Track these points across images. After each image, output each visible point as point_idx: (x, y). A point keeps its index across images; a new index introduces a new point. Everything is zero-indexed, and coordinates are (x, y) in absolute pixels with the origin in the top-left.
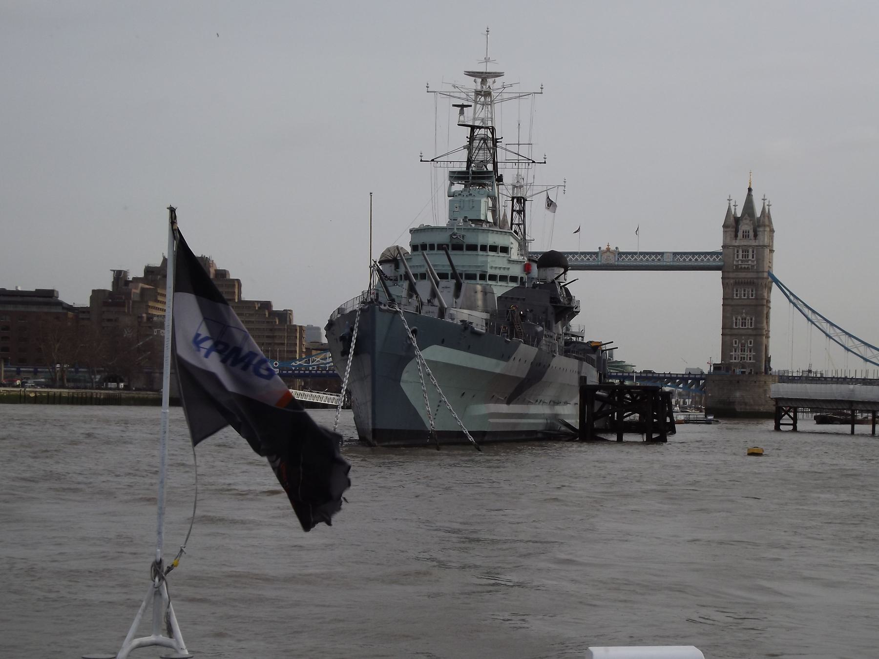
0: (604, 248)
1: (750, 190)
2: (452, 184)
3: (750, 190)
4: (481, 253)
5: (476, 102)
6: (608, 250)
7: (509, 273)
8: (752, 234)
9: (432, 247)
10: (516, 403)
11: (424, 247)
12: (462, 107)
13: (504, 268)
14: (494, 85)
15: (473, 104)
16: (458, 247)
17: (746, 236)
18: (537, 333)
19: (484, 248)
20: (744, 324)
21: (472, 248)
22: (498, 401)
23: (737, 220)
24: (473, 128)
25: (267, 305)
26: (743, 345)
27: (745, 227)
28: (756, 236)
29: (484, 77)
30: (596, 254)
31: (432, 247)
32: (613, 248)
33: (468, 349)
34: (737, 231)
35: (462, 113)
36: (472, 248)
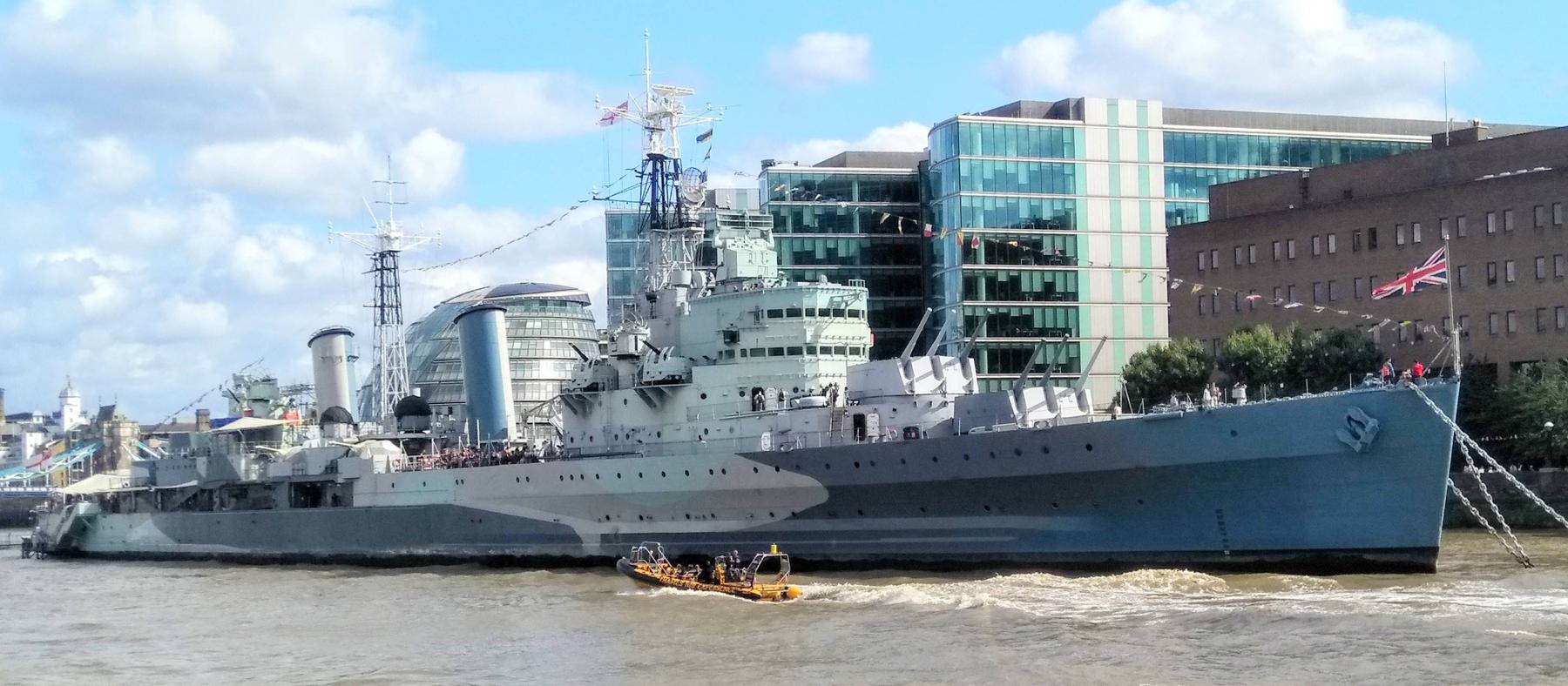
16: (839, 313)
31: (810, 313)
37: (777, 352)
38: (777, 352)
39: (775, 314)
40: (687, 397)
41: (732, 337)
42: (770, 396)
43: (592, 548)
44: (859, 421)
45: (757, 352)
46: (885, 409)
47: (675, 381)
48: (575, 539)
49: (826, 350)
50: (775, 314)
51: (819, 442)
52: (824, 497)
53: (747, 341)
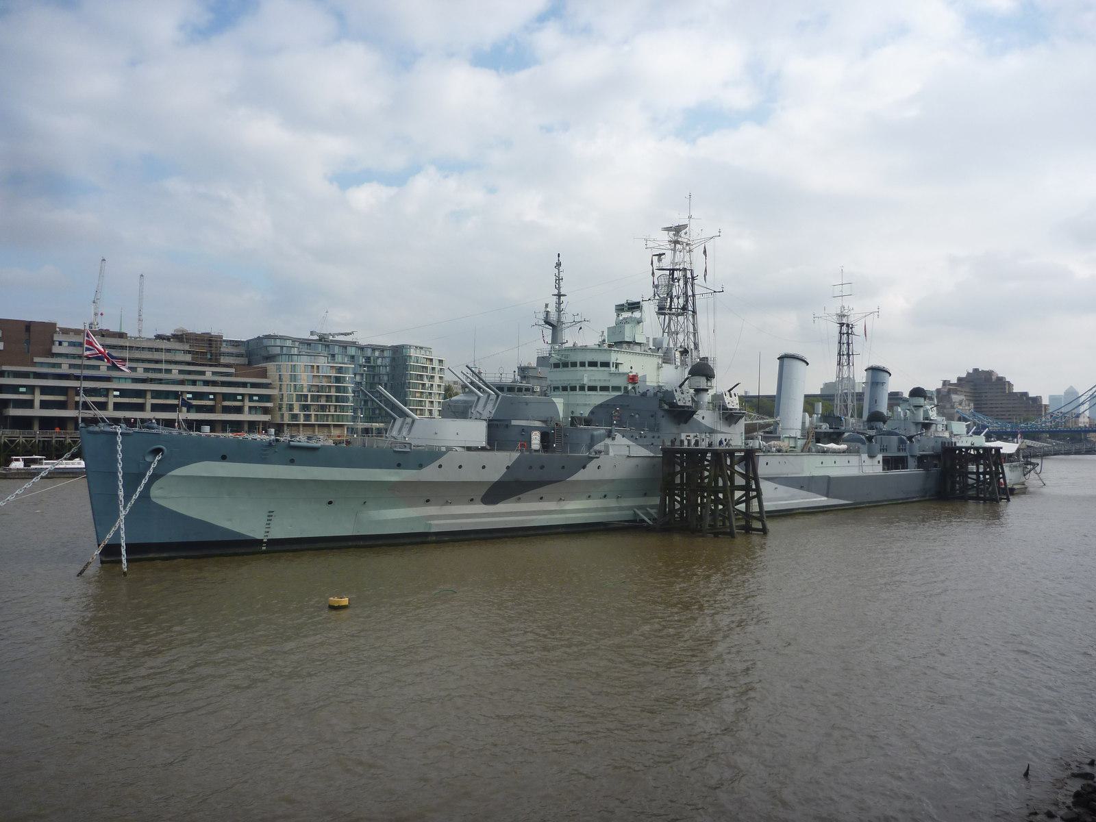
2: (618, 316)
4: (579, 368)
5: (674, 250)
7: (610, 384)
10: (517, 502)
12: (660, 255)
13: (605, 380)
15: (669, 254)
16: (565, 365)
18: (592, 437)
19: (583, 364)
21: (574, 364)
22: (447, 503)
24: (673, 270)
25: (1025, 394)
29: (678, 230)
33: (292, 462)
35: (660, 260)
36: (574, 364)
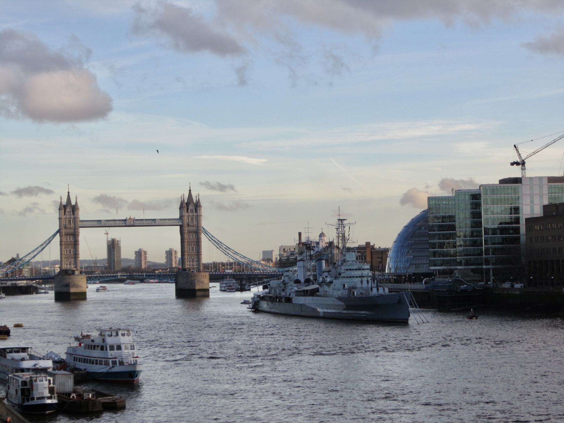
0: (128, 218)
1: (190, 191)
3: (190, 191)
6: (130, 219)
8: (194, 210)
9: (353, 270)
11: (350, 270)
14: (345, 222)
16: (360, 269)
17: (192, 211)
20: (193, 250)
21: (363, 269)
23: (187, 204)
26: (193, 260)
27: (191, 207)
28: (196, 211)
29: (342, 220)
30: (125, 220)
31: (353, 270)
32: (132, 218)
34: (188, 209)
36: (363, 269)
37: (348, 277)
38: (348, 277)
39: (347, 270)
40: (332, 286)
41: (340, 274)
42: (346, 286)
43: (321, 315)
44: (354, 293)
45: (344, 277)
46: (358, 290)
47: (331, 282)
48: (319, 312)
49: (357, 277)
50: (347, 270)
51: (346, 296)
52: (345, 307)
53: (343, 275)
